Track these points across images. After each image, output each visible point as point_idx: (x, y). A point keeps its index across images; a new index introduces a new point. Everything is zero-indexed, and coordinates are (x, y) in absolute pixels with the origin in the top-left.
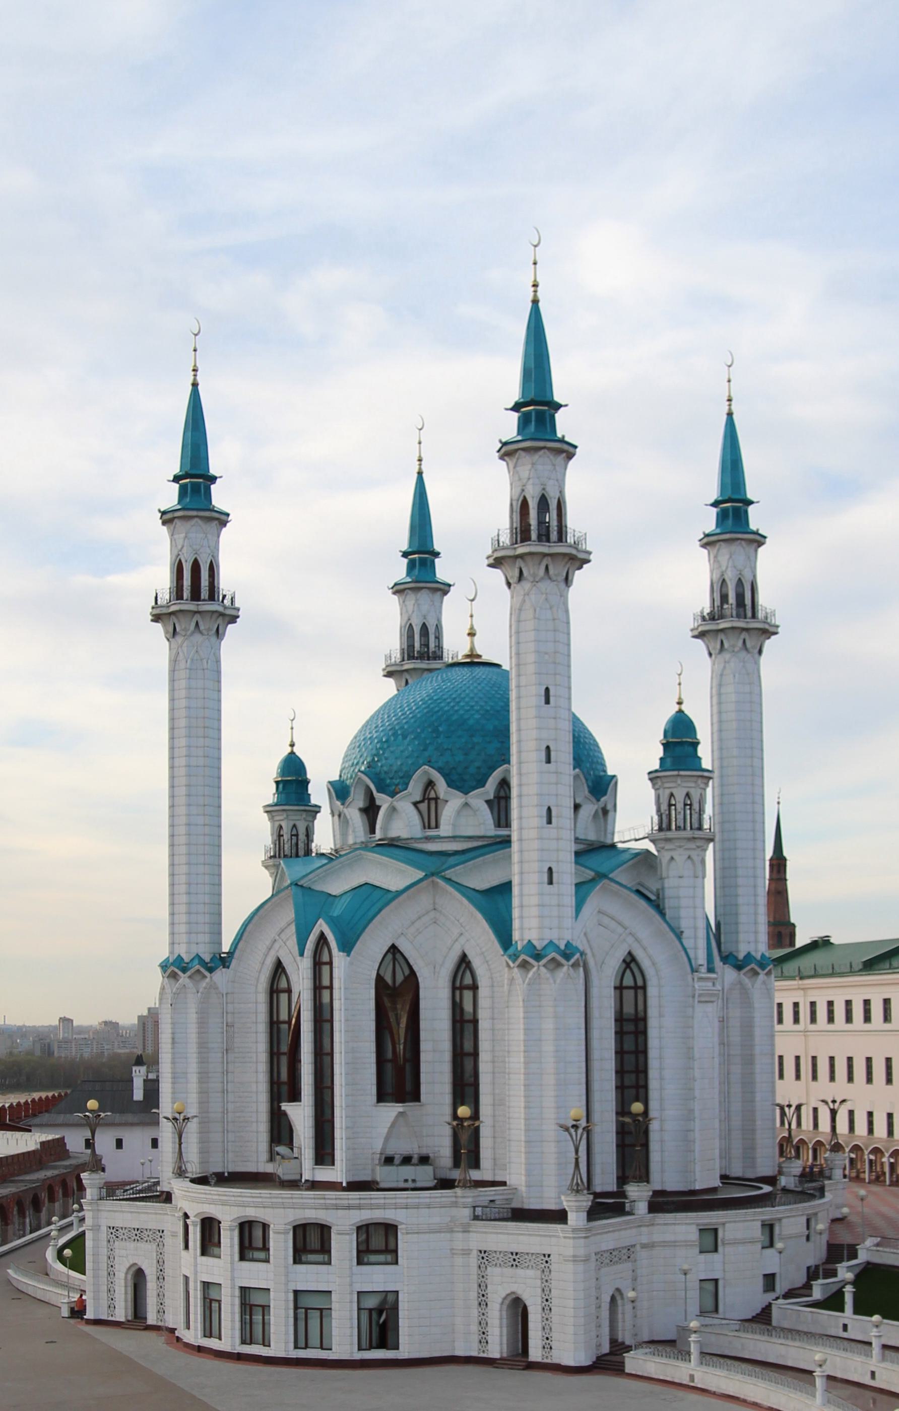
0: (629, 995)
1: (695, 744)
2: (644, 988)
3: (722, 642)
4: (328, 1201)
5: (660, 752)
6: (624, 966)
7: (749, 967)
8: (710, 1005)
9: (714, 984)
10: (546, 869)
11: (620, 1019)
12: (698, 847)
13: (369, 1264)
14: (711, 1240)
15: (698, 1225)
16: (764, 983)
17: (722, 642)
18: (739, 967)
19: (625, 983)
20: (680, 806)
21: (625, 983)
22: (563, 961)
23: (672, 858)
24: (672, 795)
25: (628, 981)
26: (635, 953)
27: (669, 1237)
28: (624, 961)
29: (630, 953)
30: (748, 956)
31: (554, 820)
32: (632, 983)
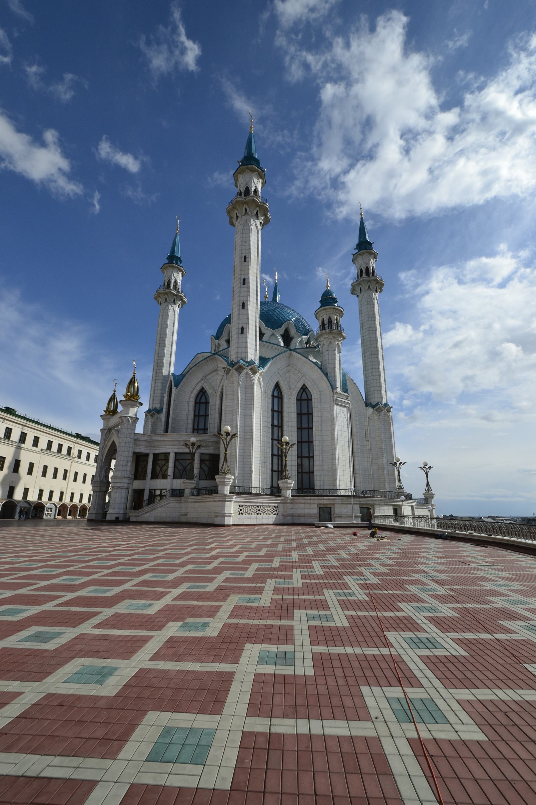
0: (304, 403)
2: (311, 400)
3: (361, 289)
5: (320, 305)
6: (302, 390)
7: (377, 407)
10: (240, 327)
15: (318, 504)
16: (385, 414)
17: (361, 289)
18: (373, 407)
20: (326, 322)
23: (324, 344)
24: (323, 320)
25: (304, 396)
26: (306, 384)
28: (302, 388)
29: (304, 385)
30: (378, 404)
31: (245, 307)
32: (306, 398)
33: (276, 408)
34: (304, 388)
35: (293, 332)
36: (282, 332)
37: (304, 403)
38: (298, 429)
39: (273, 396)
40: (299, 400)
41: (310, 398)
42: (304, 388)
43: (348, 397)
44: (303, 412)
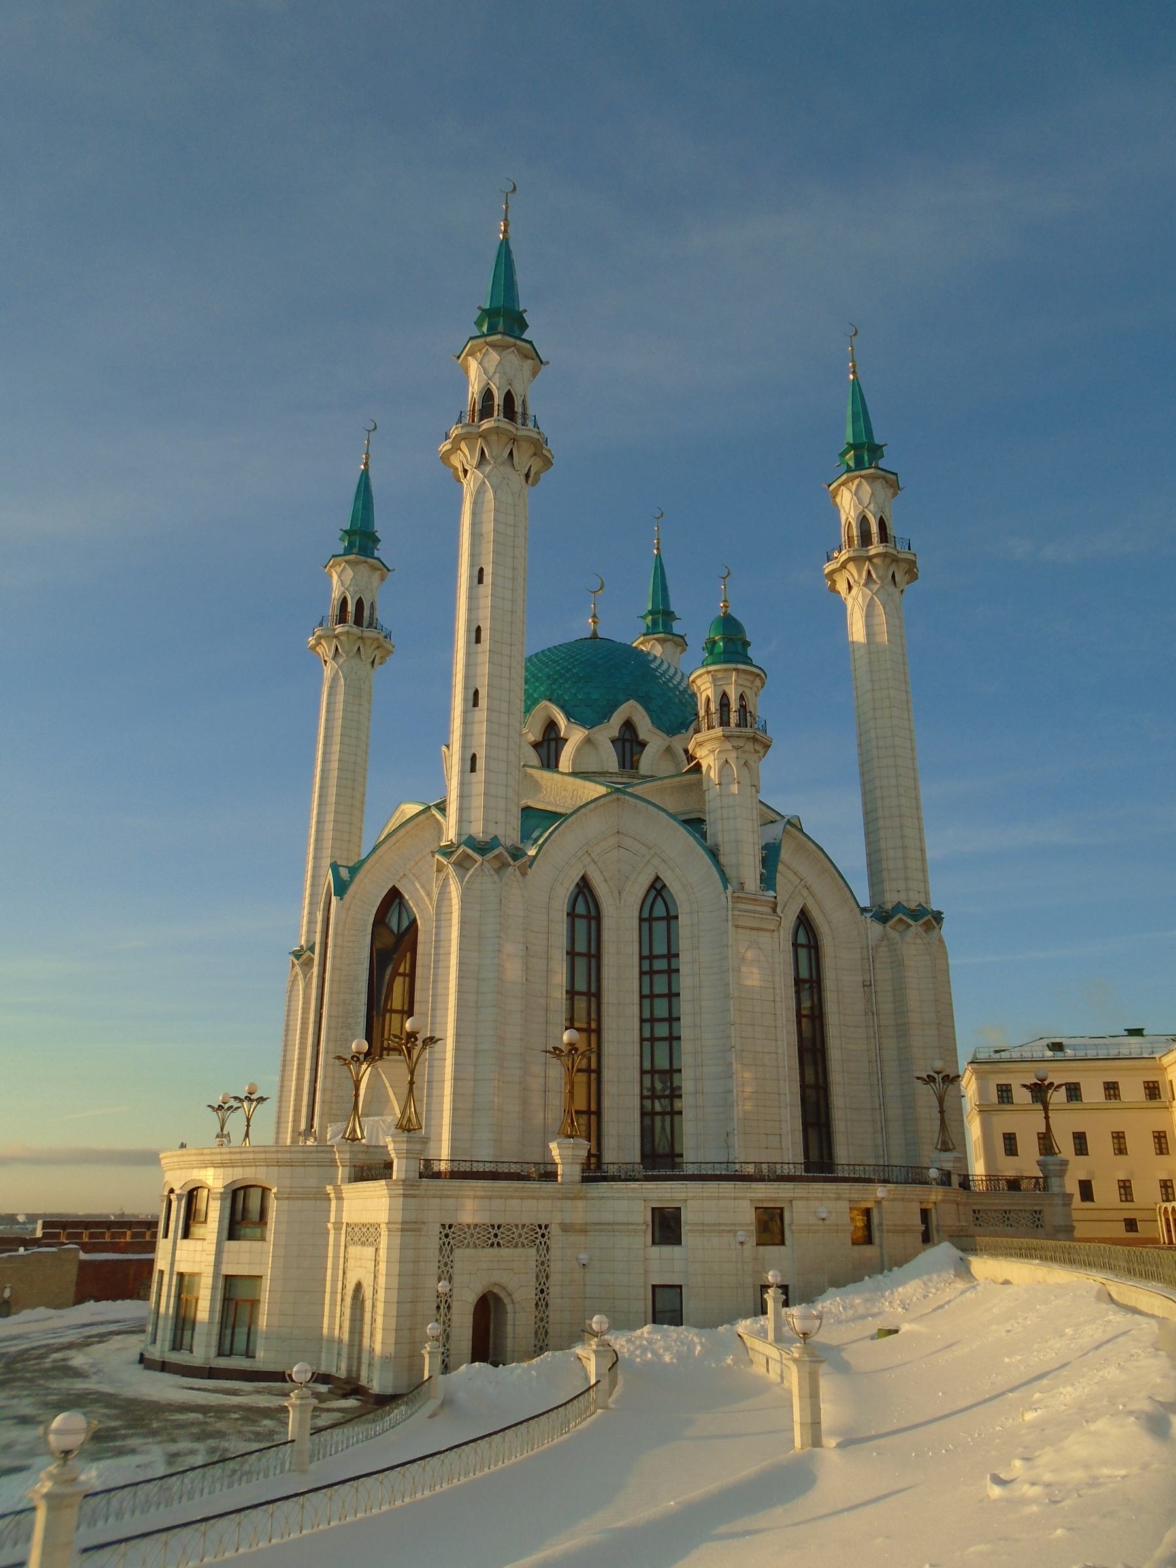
0: (660, 928)
1: (746, 644)
4: (206, 1158)
6: (653, 893)
7: (895, 919)
8: (768, 934)
9: (775, 911)
10: (469, 757)
11: (647, 957)
12: (736, 748)
13: (245, 1238)
14: (667, 1226)
19: (656, 914)
21: (656, 914)
22: (475, 856)
25: (659, 910)
27: (607, 1217)
28: (652, 886)
29: (658, 878)
30: (898, 907)
33: (581, 947)
34: (658, 886)
35: (645, 727)
36: (615, 733)
37: (660, 928)
38: (642, 997)
39: (572, 915)
40: (646, 920)
41: (672, 914)
42: (658, 889)
43: (776, 904)
44: (656, 952)
